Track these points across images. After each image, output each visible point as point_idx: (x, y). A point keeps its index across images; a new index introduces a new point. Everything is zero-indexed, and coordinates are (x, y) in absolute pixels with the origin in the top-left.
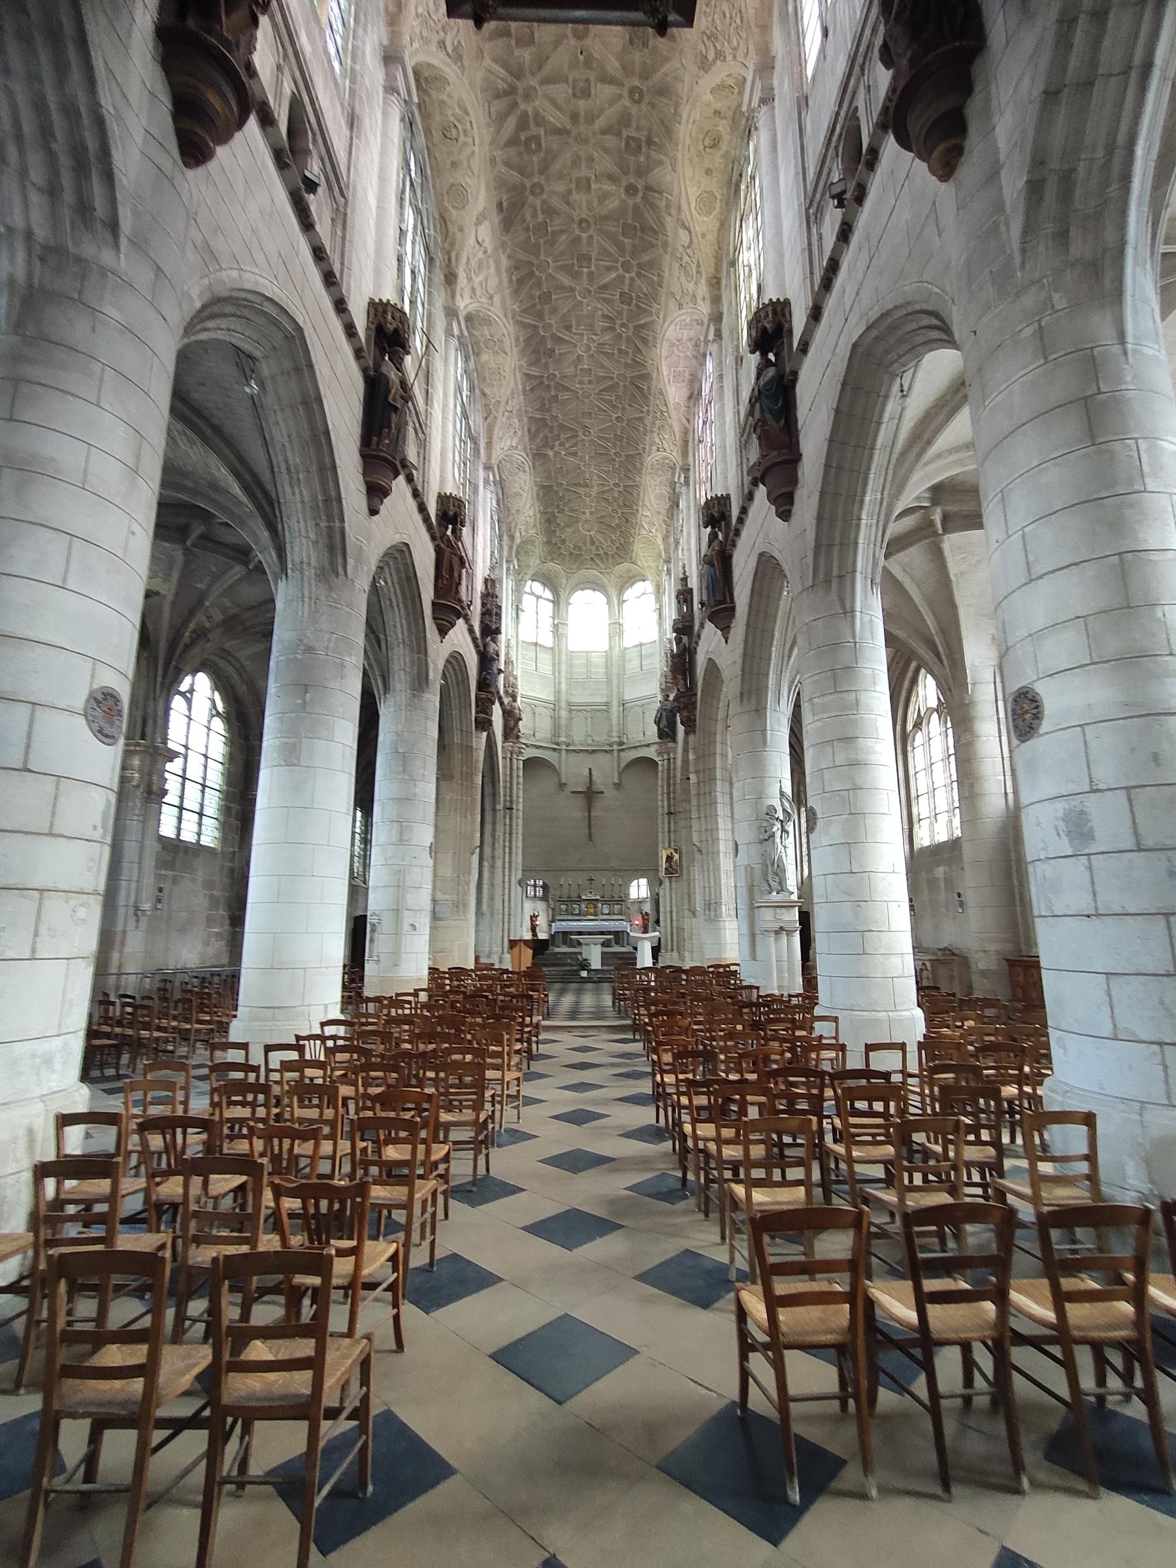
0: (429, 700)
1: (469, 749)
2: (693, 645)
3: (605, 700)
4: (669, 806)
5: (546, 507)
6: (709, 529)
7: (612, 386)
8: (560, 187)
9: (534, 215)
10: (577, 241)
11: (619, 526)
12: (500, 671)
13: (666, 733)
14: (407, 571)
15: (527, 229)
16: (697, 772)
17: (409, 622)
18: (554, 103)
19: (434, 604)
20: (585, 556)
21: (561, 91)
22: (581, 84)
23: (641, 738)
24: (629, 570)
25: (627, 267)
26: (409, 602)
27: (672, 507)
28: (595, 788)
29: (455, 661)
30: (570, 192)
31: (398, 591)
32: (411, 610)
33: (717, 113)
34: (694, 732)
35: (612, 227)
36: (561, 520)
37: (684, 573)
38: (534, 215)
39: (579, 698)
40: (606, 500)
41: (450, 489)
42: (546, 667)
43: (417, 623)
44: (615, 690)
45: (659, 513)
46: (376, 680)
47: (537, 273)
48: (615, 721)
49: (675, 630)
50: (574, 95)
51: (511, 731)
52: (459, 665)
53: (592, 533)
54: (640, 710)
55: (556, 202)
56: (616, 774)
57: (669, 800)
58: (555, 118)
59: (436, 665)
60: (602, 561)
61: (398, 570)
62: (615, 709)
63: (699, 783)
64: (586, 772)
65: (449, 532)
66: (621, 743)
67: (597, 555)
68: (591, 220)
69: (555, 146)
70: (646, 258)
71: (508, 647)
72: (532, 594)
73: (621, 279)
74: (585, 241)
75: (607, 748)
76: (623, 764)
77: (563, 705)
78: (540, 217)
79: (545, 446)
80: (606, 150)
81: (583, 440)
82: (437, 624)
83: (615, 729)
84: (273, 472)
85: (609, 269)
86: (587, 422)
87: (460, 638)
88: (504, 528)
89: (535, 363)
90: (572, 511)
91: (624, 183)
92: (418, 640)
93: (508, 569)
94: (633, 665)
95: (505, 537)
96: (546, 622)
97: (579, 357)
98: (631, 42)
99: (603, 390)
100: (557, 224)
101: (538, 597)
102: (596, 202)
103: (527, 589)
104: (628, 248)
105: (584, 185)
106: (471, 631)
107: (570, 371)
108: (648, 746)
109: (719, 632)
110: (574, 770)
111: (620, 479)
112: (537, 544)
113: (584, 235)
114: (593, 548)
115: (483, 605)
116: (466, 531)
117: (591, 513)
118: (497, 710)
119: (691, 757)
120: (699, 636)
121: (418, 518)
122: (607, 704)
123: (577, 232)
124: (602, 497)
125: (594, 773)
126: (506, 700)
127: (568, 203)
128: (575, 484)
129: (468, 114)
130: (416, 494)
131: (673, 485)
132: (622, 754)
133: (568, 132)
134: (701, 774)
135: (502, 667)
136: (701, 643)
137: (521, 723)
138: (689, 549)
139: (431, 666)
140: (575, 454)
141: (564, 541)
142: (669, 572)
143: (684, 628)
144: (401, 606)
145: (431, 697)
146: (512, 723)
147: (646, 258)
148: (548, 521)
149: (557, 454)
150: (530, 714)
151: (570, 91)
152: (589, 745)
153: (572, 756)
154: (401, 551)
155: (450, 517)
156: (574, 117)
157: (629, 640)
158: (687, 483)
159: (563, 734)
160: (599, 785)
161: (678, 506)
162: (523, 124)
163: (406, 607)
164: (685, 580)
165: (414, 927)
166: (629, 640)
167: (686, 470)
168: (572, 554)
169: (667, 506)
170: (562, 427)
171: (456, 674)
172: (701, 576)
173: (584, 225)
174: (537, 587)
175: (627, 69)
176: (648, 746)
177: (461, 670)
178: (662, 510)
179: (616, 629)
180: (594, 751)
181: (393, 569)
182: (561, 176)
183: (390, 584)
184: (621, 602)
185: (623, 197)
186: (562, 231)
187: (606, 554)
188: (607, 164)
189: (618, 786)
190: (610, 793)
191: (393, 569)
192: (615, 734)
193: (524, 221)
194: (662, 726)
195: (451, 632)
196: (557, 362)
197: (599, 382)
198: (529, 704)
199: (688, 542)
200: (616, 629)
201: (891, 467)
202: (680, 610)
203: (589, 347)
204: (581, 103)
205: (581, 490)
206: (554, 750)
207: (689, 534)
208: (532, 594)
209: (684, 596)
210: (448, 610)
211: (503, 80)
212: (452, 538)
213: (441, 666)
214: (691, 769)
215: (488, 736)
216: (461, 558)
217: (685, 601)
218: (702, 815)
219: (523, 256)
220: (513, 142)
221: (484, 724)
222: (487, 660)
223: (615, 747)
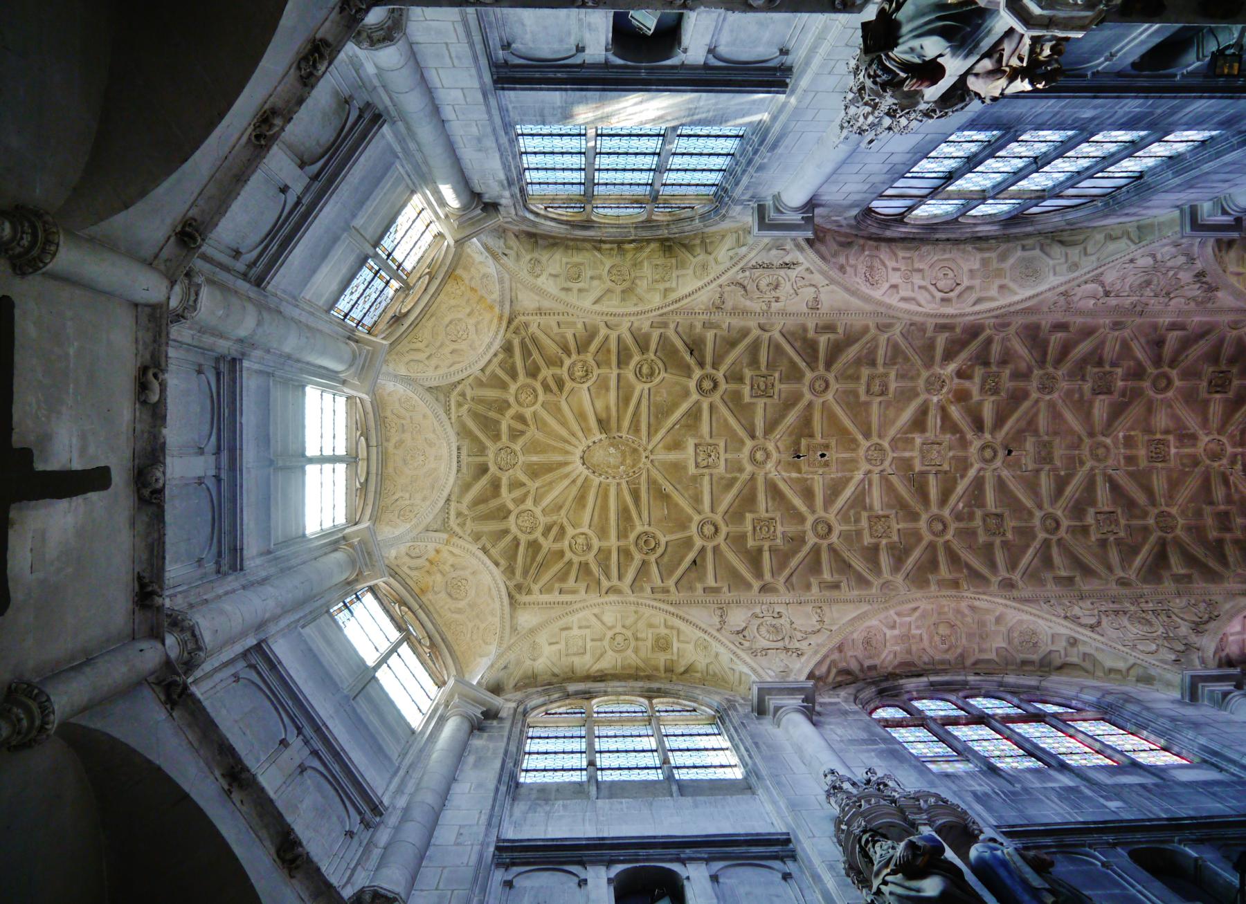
7: (1131, 504)
40: (748, 500)
53: (578, 468)
60: (477, 502)
67: (496, 486)
79: (983, 359)
81: (964, 443)
86: (1028, 453)
89: (1213, 357)
90: (694, 415)
97: (1194, 438)
99: (1115, 487)
107: (1161, 420)
112: (613, 305)
140: (919, 423)
149: (935, 383)
168: (503, 406)
170: (1017, 397)
196: (1189, 397)
197: (1131, 475)
203: (1215, 456)
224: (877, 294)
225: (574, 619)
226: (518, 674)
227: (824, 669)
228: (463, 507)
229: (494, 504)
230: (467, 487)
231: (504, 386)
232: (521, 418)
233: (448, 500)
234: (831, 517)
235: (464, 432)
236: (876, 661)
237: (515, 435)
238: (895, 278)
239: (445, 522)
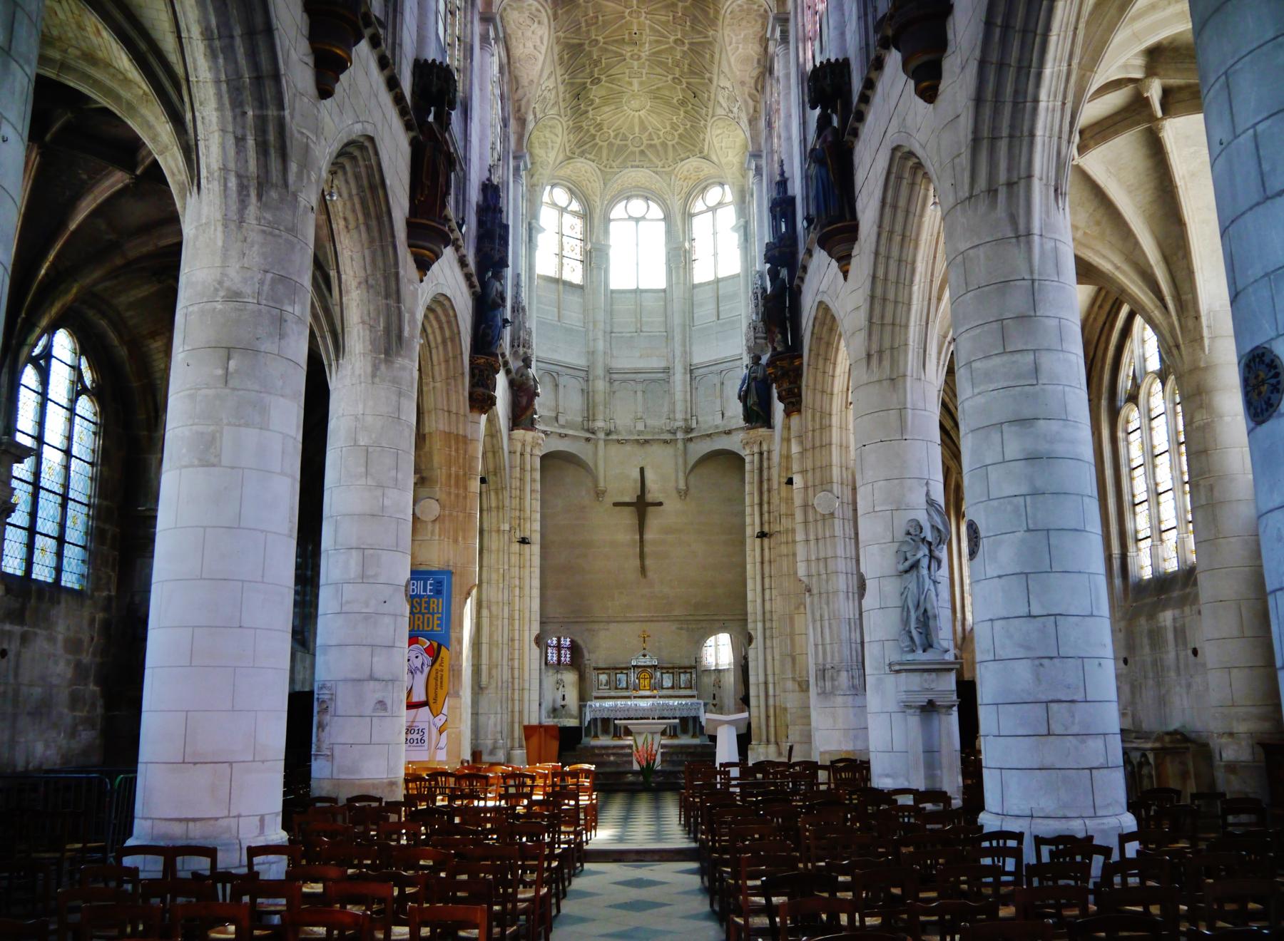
0: (403, 368)
1: (463, 441)
2: (796, 281)
3: (663, 364)
4: (762, 524)
5: (573, 75)
6: (818, 111)
11: (683, 103)
12: (506, 321)
13: (757, 414)
14: (370, 176)
16: (803, 472)
17: (373, 254)
19: (410, 225)
20: (632, 148)
23: (718, 421)
24: (698, 169)
26: (374, 223)
27: (762, 75)
28: (650, 497)
29: (440, 304)
31: (358, 206)
32: (376, 234)
34: (799, 411)
36: (596, 92)
37: (782, 173)
39: (626, 360)
40: (660, 64)
41: (431, 54)
42: (573, 317)
43: (385, 255)
44: (678, 353)
45: (743, 83)
46: (323, 338)
48: (679, 396)
49: (768, 259)
51: (522, 414)
52: (447, 315)
54: (716, 380)
56: (681, 476)
57: (761, 515)
59: (413, 315)
61: (357, 177)
62: (679, 377)
63: (806, 488)
64: (637, 474)
65: (431, 118)
66: (689, 430)
67: (651, 146)
71: (517, 285)
72: (554, 205)
75: (668, 437)
76: (692, 460)
77: (600, 371)
82: (413, 253)
83: (679, 407)
84: (179, 37)
87: (449, 276)
88: (510, 107)
92: (386, 278)
93: (517, 169)
94: (705, 312)
95: (512, 122)
96: (574, 249)
101: (563, 210)
103: (546, 198)
106: (463, 262)
108: (729, 433)
109: (834, 263)
110: (617, 470)
111: (685, 34)
114: (645, 136)
115: (480, 223)
116: (455, 116)
117: (641, 83)
118: (501, 380)
119: (795, 448)
120: (805, 269)
121: (386, 98)
122: (667, 370)
124: (656, 60)
125: (649, 475)
126: (515, 364)
128: (616, 41)
130: (383, 63)
131: (764, 42)
132: (691, 446)
134: (810, 474)
135: (508, 315)
136: (807, 278)
137: (537, 401)
138: (789, 138)
139: (407, 316)
141: (599, 127)
142: (758, 171)
143: (783, 259)
144: (363, 228)
145: (407, 362)
146: (524, 401)
148: (577, 96)
150: (549, 386)
152: (640, 433)
153: (614, 450)
154: (362, 147)
155: (432, 96)
157: (702, 273)
158: (785, 39)
159: (600, 417)
160: (654, 493)
161: (771, 71)
163: (368, 228)
164: (783, 184)
165: (382, 704)
166: (702, 273)
167: (783, 20)
168: (611, 145)
169: (755, 73)
171: (441, 328)
172: (806, 177)
174: (561, 196)
176: (729, 433)
177: (449, 322)
178: (747, 79)
179: (680, 257)
180: (646, 441)
181: (350, 174)
183: (345, 195)
184: (688, 216)
187: (664, 145)
189: (684, 494)
190: (672, 505)
191: (350, 174)
192: (679, 416)
194: (750, 402)
195: (435, 267)
198: (549, 373)
199: (788, 127)
200: (680, 257)
201: (1082, 26)
202: (775, 229)
205: (627, 51)
206: (588, 440)
207: (789, 116)
208: (554, 205)
209: (782, 207)
210: (428, 234)
212: (435, 127)
213: (420, 316)
214: (795, 467)
215: (489, 420)
216: (449, 155)
217: (784, 215)
218: (812, 537)
221: (482, 401)
222: (487, 306)
223: (680, 435)
224: (541, 58)
225: (717, 146)
226: (738, 174)
227: (751, 103)
228: (660, 164)
229: (659, 148)
230: (650, 160)
231: (601, 147)
232: (616, 137)
233: (656, 173)
234: (672, 38)
235: (623, 166)
236: (756, 57)
237: (625, 138)
238: (530, 44)
239: (666, 173)
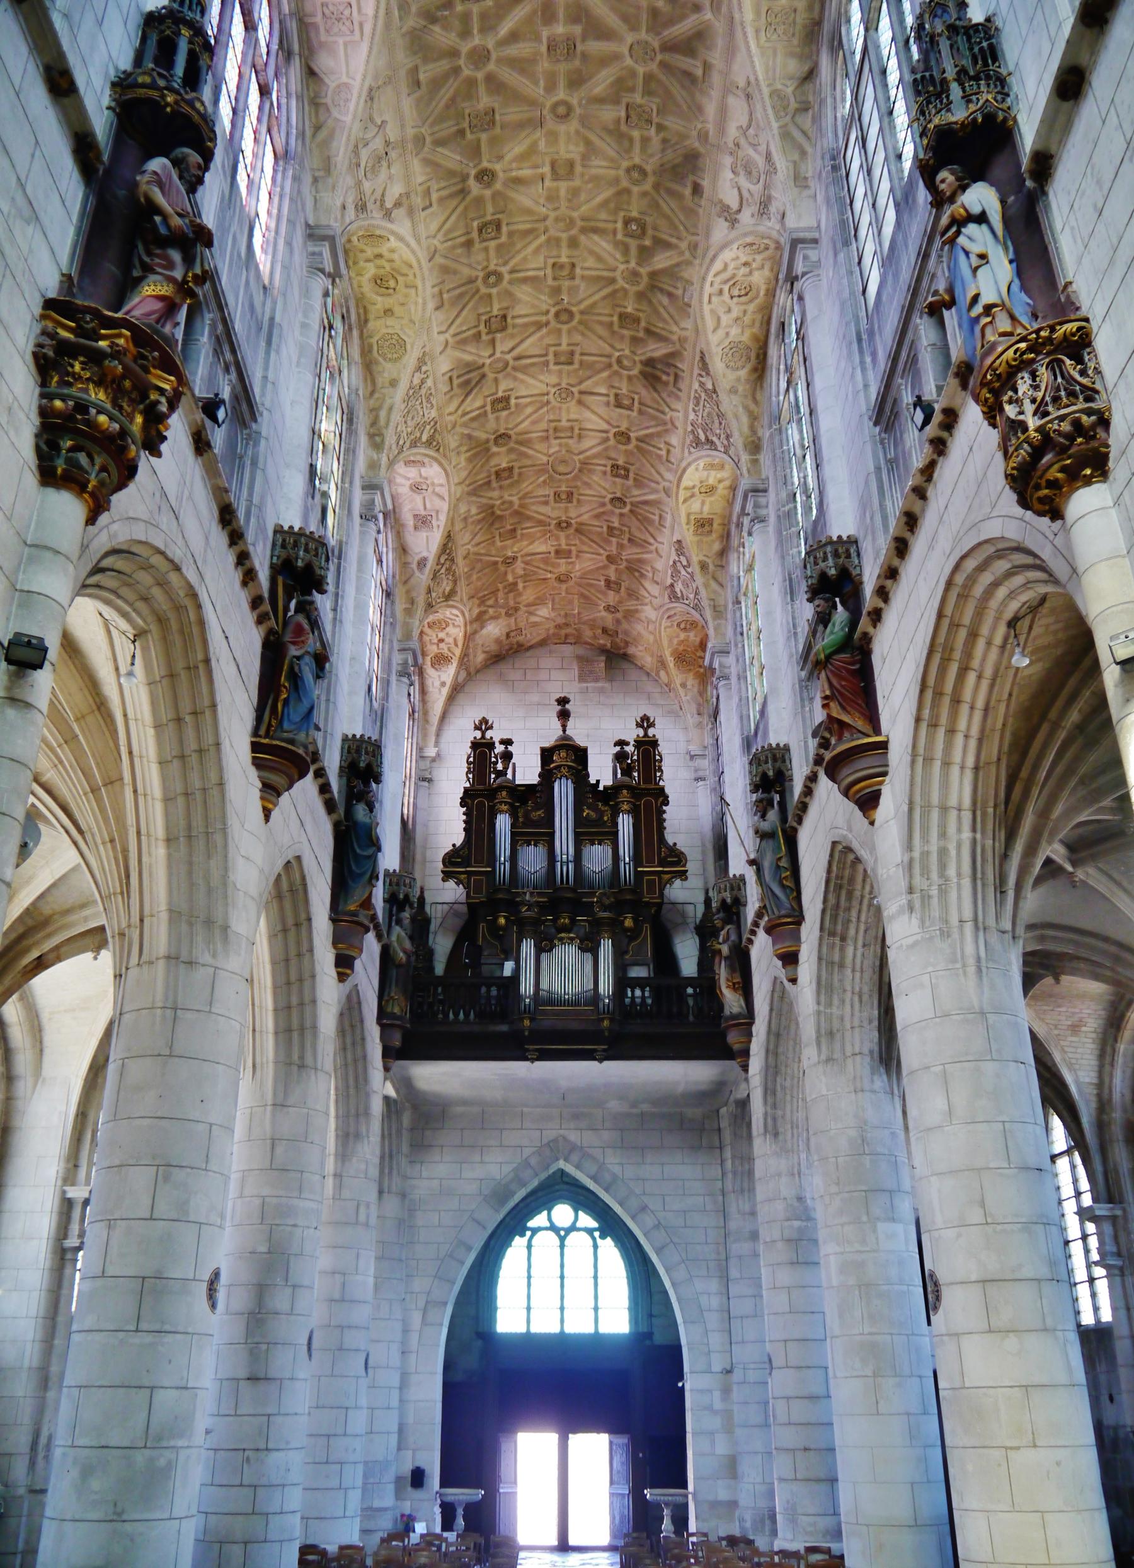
8: (599, 166)
9: (645, 140)
10: (576, 81)
15: (660, 128)
18: (599, 259)
21: (588, 265)
22: (565, 272)
25: (480, 56)
30: (585, 157)
33: (388, 312)
35: (512, 113)
38: (645, 140)
47: (656, 45)
50: (573, 265)
55: (607, 147)
58: (603, 245)
68: (550, 124)
69: (603, 216)
70: (446, 93)
73: (487, 27)
74: (562, 83)
78: (636, 134)
80: (528, 211)
85: (514, 37)
91: (498, 186)
98: (504, 317)
100: (610, 114)
102: (542, 145)
104: (482, 89)
105: (562, 170)
113: (561, 94)
123: (574, 102)
127: (588, 143)
129: (712, 311)
133: (584, 230)
147: (446, 93)
151: (578, 271)
156: (573, 243)
162: (645, 254)
173: (562, 110)
175: (509, 294)
182: (595, 179)
185: (497, 167)
186: (600, 100)
188: (523, 198)
193: (665, 141)
204: (564, 259)
211: (661, 303)
219: (676, 89)
220: (661, 244)
